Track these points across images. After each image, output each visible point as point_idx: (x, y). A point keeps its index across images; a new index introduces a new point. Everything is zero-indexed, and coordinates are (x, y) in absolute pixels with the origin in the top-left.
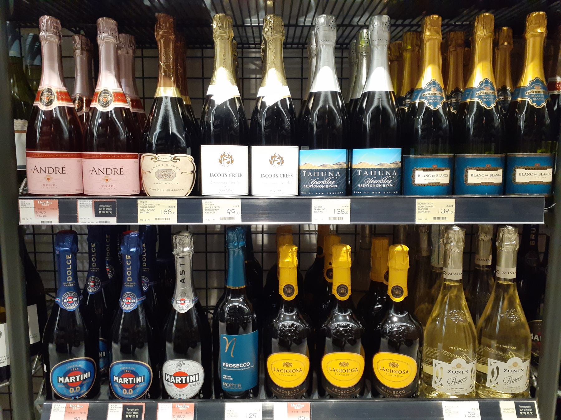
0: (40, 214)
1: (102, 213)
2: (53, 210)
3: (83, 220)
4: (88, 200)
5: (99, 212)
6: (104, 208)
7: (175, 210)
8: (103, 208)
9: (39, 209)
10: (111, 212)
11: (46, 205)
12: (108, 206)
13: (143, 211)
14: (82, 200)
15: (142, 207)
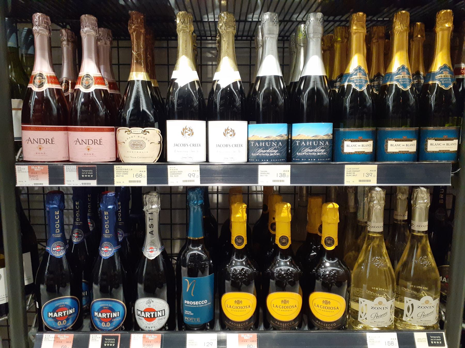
0: (33, 178)
1: (84, 176)
2: (44, 174)
3: (69, 183)
4: (73, 166)
5: (82, 175)
6: (86, 172)
7: (145, 174)
8: (85, 172)
9: (32, 173)
10: (92, 176)
11: (38, 170)
12: (89, 171)
13: (118, 175)
14: (68, 166)
15: (118, 172)
